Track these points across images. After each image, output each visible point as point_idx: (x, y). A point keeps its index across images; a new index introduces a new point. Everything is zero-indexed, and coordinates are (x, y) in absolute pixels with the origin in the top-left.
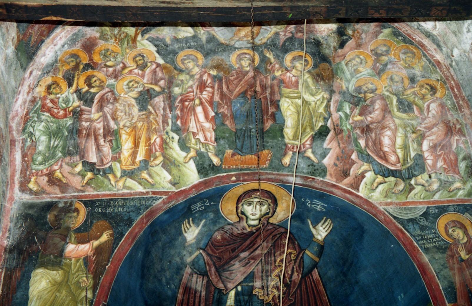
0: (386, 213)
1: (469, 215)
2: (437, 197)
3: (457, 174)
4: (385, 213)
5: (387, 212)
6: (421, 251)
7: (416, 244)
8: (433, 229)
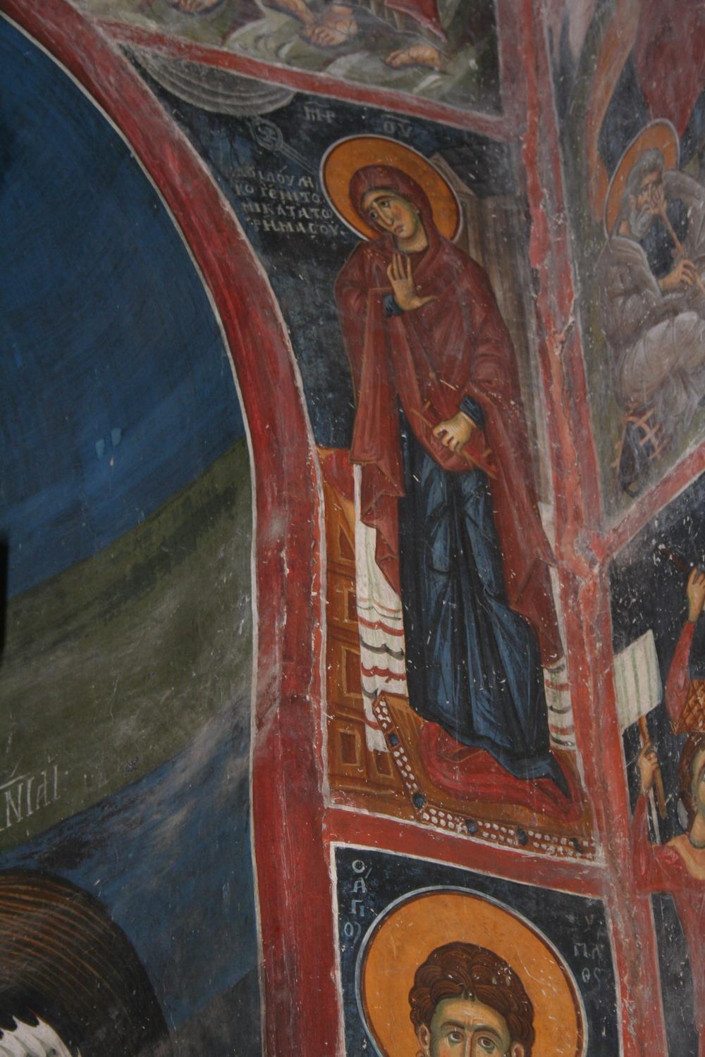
0: (132, 69)
1: (444, 164)
2: (337, 71)
3: (428, 16)
4: (124, 68)
5: (137, 65)
6: (243, 236)
7: (228, 207)
8: (305, 174)
